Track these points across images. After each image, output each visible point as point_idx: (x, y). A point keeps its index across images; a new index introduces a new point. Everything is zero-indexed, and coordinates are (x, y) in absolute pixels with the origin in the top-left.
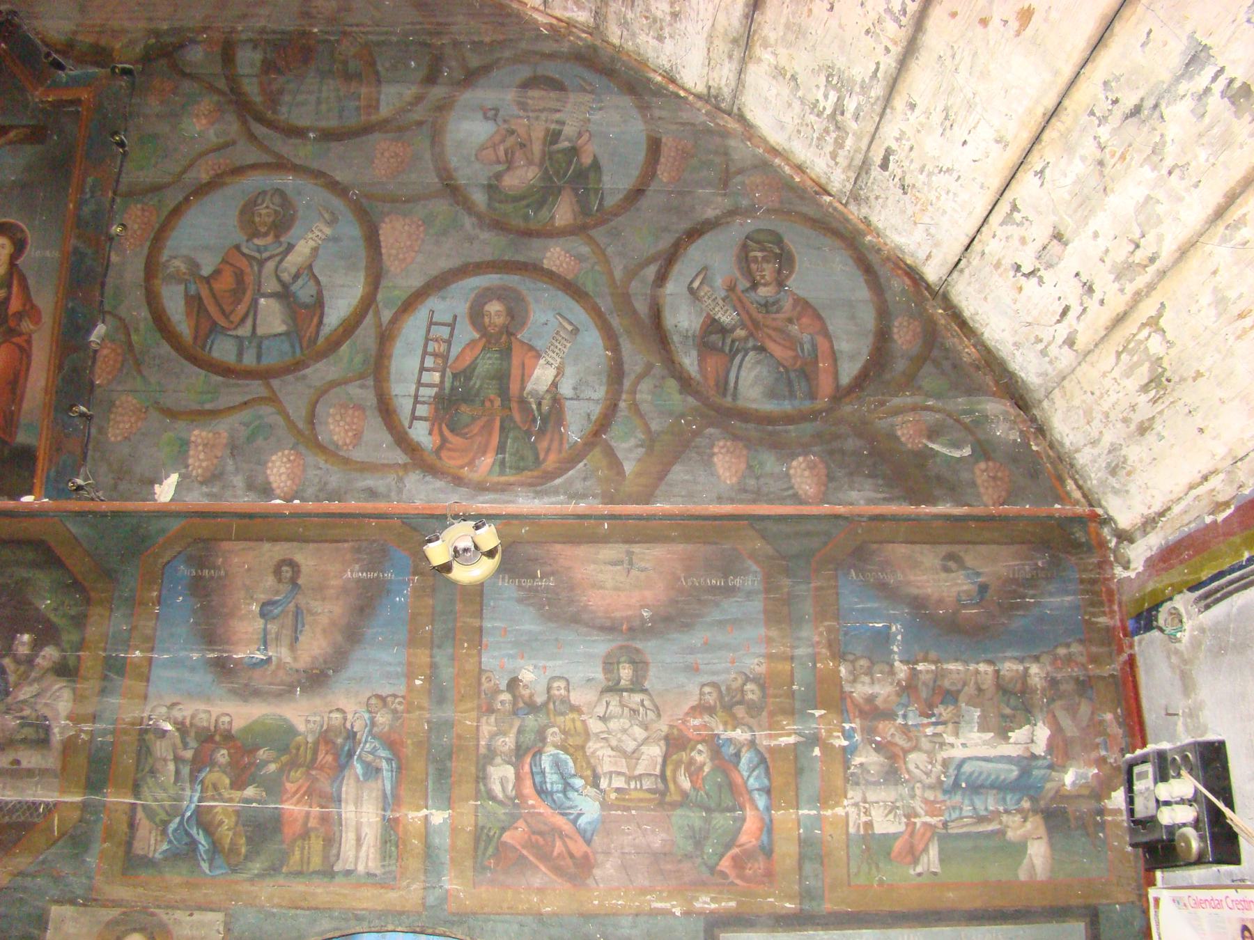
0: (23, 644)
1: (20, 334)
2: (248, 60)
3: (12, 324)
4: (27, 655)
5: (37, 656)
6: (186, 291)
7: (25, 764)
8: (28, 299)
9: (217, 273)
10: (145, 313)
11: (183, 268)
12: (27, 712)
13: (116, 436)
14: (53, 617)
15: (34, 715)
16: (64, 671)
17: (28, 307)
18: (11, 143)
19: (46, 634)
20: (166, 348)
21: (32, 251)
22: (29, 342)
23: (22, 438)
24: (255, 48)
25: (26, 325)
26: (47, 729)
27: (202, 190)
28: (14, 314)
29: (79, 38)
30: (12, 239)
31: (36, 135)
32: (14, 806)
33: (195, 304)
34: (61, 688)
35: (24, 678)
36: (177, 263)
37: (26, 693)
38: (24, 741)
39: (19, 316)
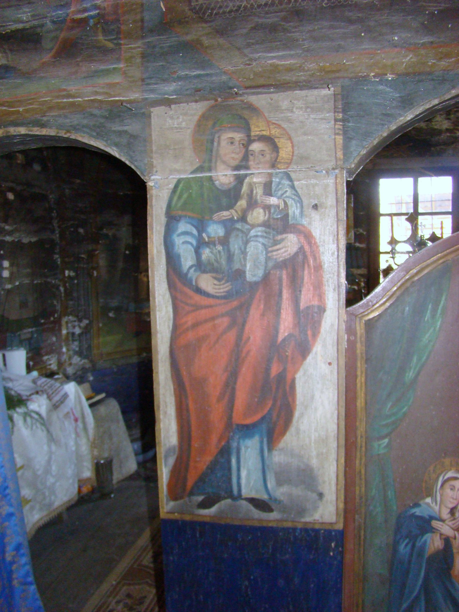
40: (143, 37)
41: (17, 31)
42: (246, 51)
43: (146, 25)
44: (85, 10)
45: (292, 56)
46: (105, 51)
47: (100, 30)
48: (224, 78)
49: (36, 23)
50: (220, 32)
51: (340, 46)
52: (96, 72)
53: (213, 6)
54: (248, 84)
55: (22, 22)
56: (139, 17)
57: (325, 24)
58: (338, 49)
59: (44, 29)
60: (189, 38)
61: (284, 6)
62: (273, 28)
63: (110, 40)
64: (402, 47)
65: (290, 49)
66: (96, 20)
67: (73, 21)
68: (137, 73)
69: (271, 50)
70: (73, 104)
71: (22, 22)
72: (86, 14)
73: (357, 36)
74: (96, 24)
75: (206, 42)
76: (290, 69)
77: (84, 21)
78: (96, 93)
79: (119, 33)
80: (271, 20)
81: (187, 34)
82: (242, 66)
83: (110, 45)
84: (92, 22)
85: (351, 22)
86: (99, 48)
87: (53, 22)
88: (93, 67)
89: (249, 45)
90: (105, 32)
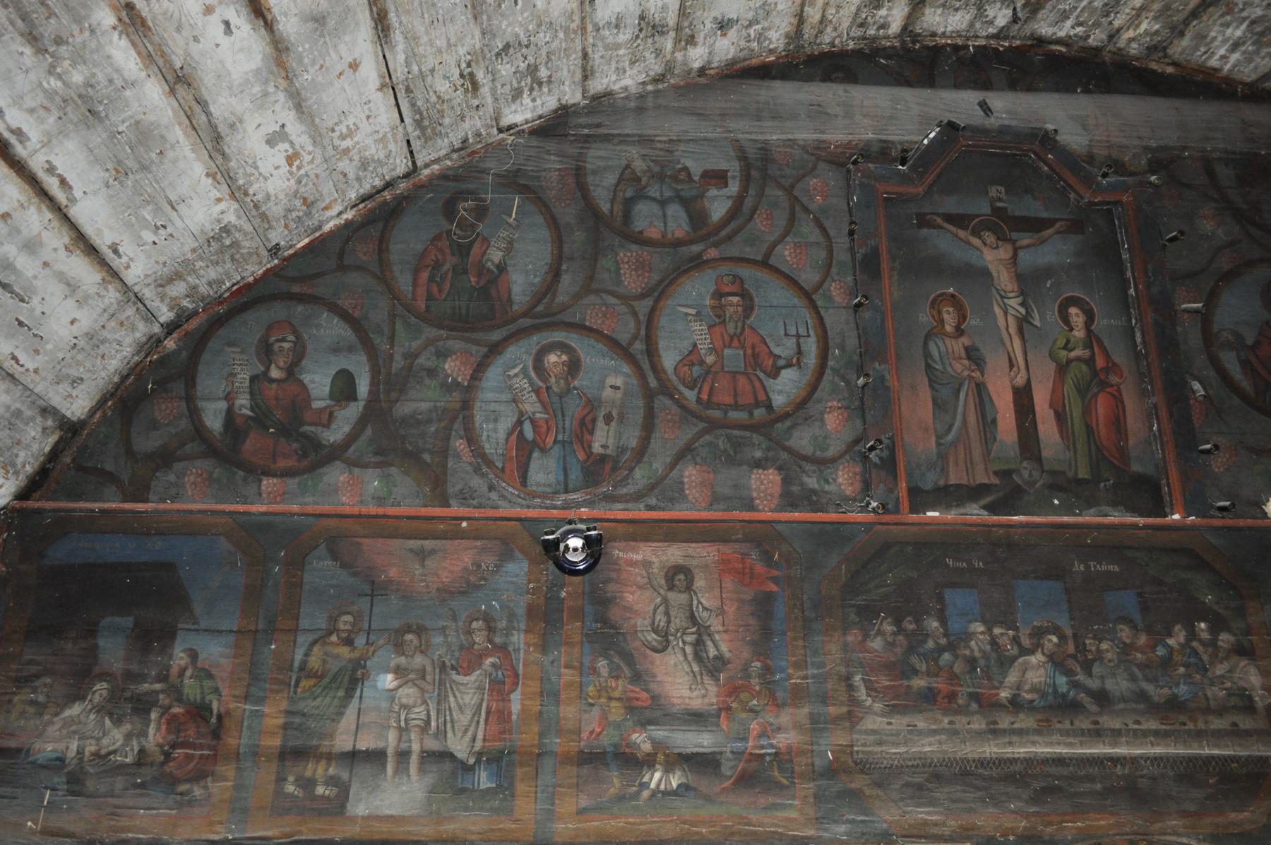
0: (1203, 630)
1: (1112, 386)
2: (1225, 174)
3: (1103, 377)
4: (1209, 640)
5: (1218, 640)
6: (1238, 356)
7: (1242, 726)
8: (1107, 357)
9: (1257, 343)
10: (1212, 373)
11: (1231, 338)
12: (1228, 685)
13: (1219, 468)
14: (1216, 607)
15: (1235, 687)
16: (1243, 651)
17: (1110, 365)
18: (1058, 233)
19: (1218, 625)
20: (1236, 401)
21: (1100, 323)
22: (1119, 390)
23: (1136, 467)
24: (1226, 165)
25: (1114, 379)
26: (1250, 698)
27: (1228, 277)
28: (1102, 369)
29: (1096, 151)
30: (1082, 309)
31: (1076, 226)
32: (1246, 760)
33: (1245, 365)
34: (1245, 667)
35: (1215, 658)
36: (1225, 334)
37: (1220, 670)
38: (1234, 707)
39: (1107, 370)
40: (814, 780)
41: (697, 754)
42: (901, 804)
43: (816, 769)
44: (762, 747)
45: (936, 813)
46: (782, 787)
47: (776, 767)
48: (885, 826)
49: (717, 750)
50: (879, 785)
51: (971, 808)
52: (774, 804)
53: (870, 760)
54: (904, 833)
55: (703, 747)
56: (809, 761)
57: (959, 788)
58: (970, 810)
59: (724, 756)
60: (853, 786)
61: (926, 769)
62: (920, 787)
63: (785, 778)
64: (1017, 813)
65: (934, 806)
66: (772, 758)
67: (751, 754)
68: (811, 812)
69: (918, 806)
70: (755, 833)
71: (703, 747)
72: (763, 751)
73: (983, 801)
74: (771, 761)
75: (868, 792)
76: (936, 824)
77: (763, 755)
78: (779, 826)
79: (793, 772)
80: (918, 779)
81: (851, 782)
82: (897, 818)
83: (785, 782)
84: (768, 758)
85: (977, 788)
86: (776, 783)
87: (732, 752)
88: (771, 800)
89: (902, 799)
90: (781, 770)
